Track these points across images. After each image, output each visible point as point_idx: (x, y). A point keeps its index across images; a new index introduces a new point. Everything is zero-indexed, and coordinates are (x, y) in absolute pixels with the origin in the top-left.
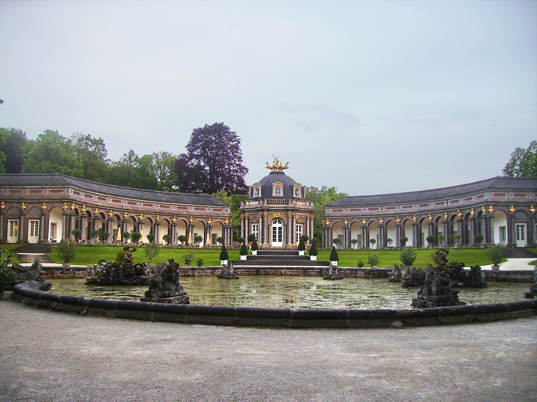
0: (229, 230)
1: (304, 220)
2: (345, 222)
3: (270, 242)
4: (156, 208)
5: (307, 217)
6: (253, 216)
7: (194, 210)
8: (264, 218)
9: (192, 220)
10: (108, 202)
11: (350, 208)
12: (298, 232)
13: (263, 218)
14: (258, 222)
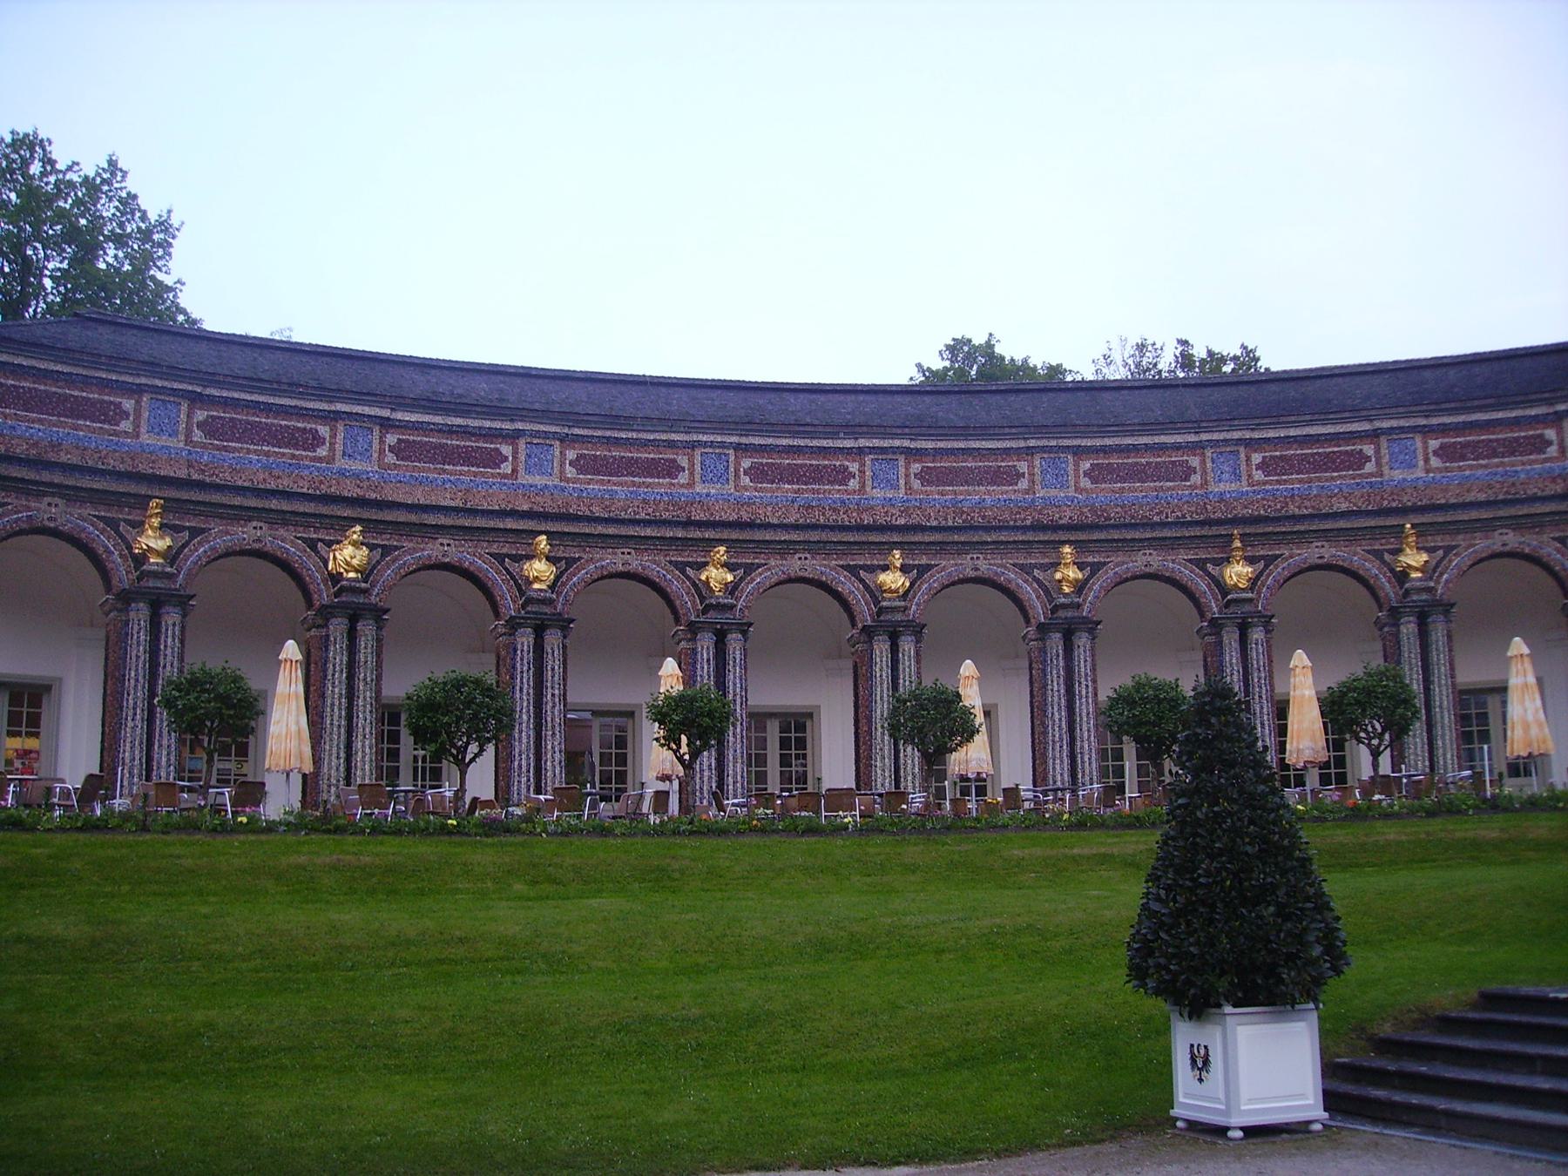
4: (1053, 492)
7: (1435, 462)
9: (1413, 558)
10: (525, 479)
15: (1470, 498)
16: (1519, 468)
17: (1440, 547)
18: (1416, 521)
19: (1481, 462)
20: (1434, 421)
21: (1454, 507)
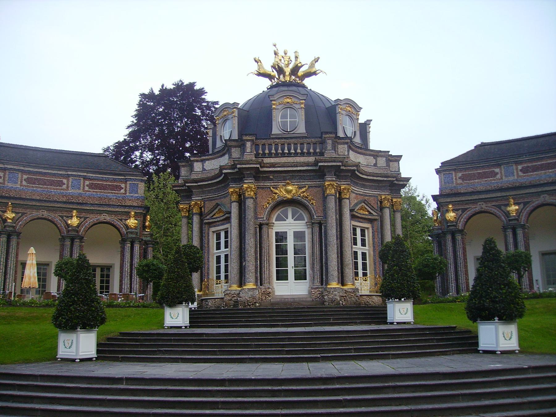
0: (137, 247)
1: (372, 208)
2: (509, 209)
3: (265, 281)
5: (381, 202)
6: (214, 203)
7: (24, 183)
8: (245, 198)
9: (10, 215)
11: (521, 163)
12: (359, 248)
13: (241, 202)
14: (228, 220)
15: (34, 197)
16: (52, 190)
17: (21, 213)
18: (13, 202)
19: (40, 186)
20: (26, 169)
21: (28, 199)
